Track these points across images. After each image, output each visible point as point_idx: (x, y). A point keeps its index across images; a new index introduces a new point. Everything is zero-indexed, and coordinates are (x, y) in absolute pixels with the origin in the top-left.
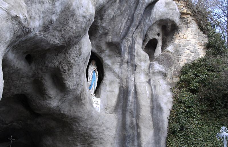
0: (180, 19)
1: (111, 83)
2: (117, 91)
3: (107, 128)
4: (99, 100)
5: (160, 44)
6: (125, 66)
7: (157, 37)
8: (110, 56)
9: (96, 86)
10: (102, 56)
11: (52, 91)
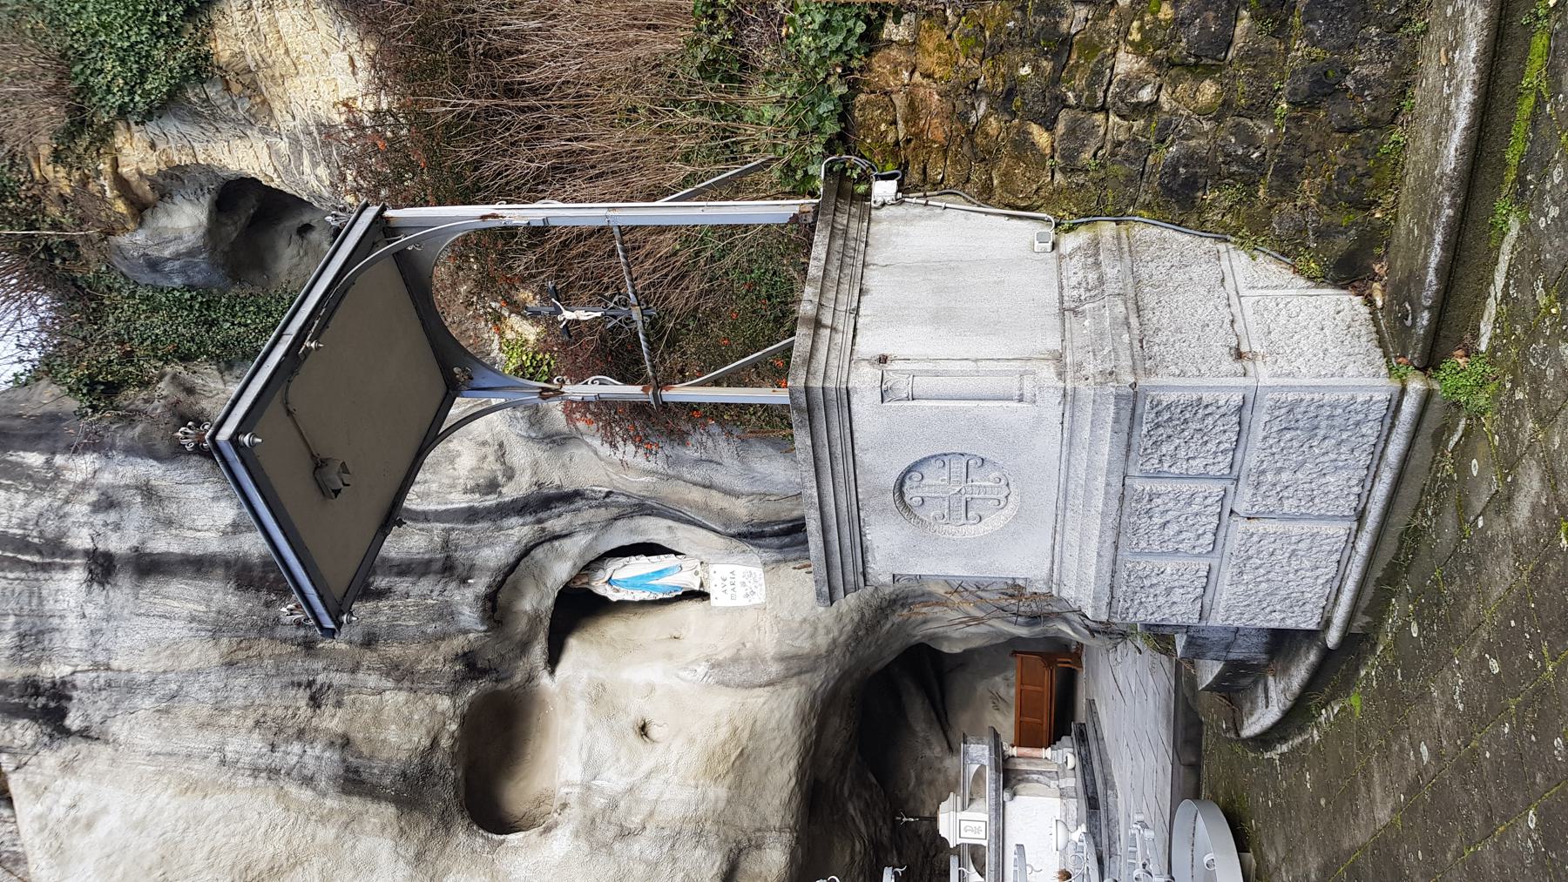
0: (171, 197)
6: (555, 525)
8: (539, 580)
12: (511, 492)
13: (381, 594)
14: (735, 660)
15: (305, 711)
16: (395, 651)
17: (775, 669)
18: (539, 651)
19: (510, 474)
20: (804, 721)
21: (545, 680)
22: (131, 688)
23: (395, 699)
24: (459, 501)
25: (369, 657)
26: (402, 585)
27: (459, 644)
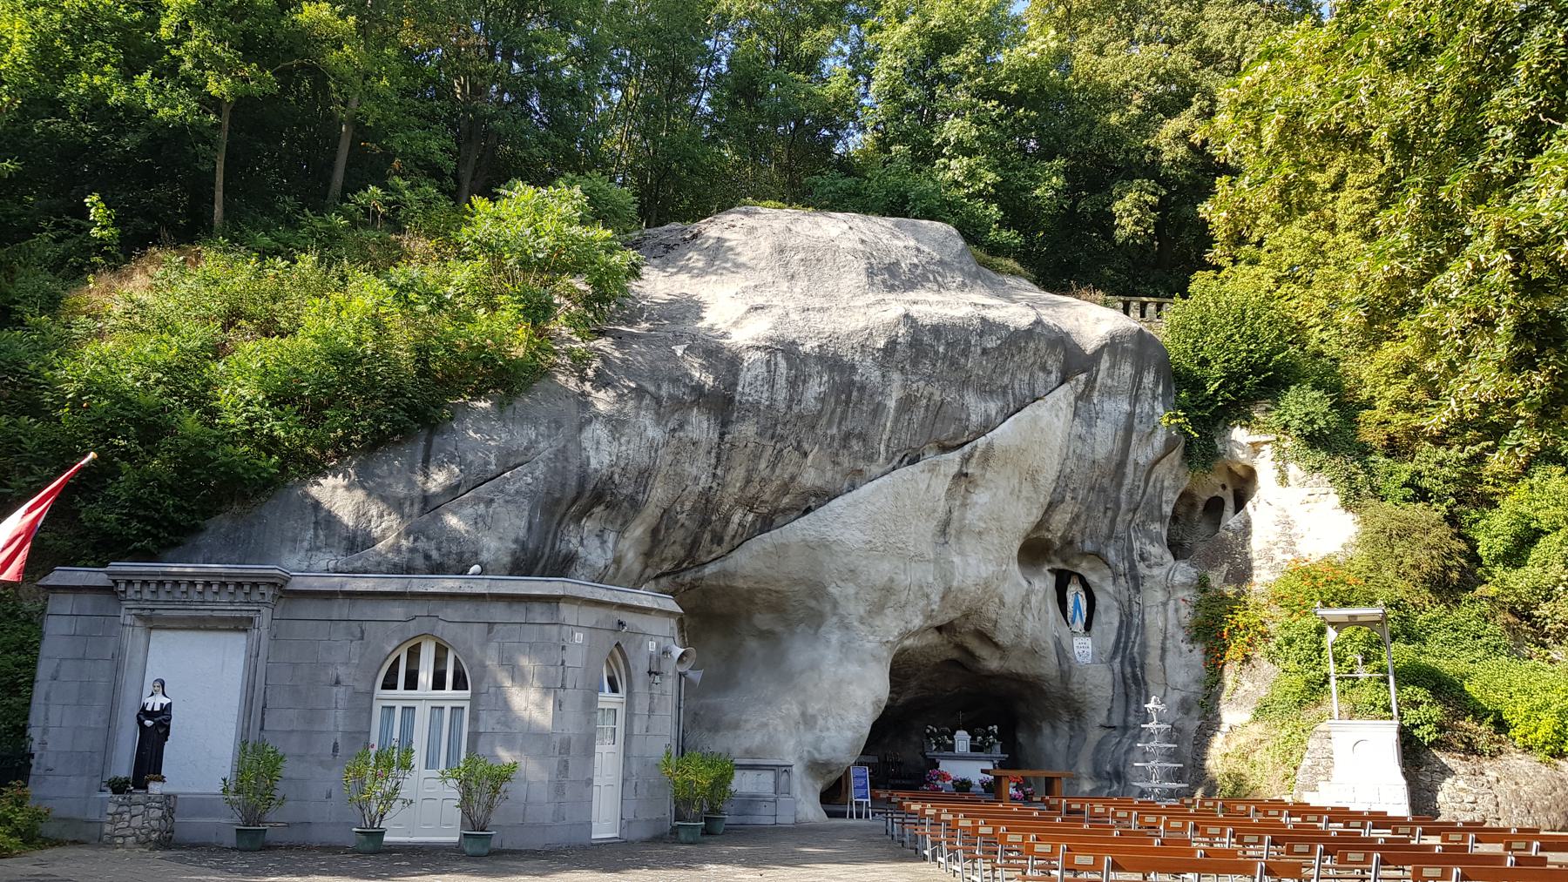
1: (1107, 609)
2: (1116, 624)
3: (1096, 687)
4: (1088, 641)
5: (1230, 504)
6: (1122, 580)
7: (1219, 493)
8: (1092, 569)
9: (1085, 613)
10: (1080, 571)
11: (983, 652)
12: (1142, 568)
13: (1105, 513)
14: (1064, 650)
15: (1072, 487)
16: (1083, 517)
17: (1066, 667)
18: (1060, 566)
19: (1149, 567)
20: (1038, 677)
21: (1047, 567)
22: (1090, 426)
23: (1068, 517)
24: (1137, 545)
25: (1083, 508)
26: (1107, 521)
27: (1078, 539)
